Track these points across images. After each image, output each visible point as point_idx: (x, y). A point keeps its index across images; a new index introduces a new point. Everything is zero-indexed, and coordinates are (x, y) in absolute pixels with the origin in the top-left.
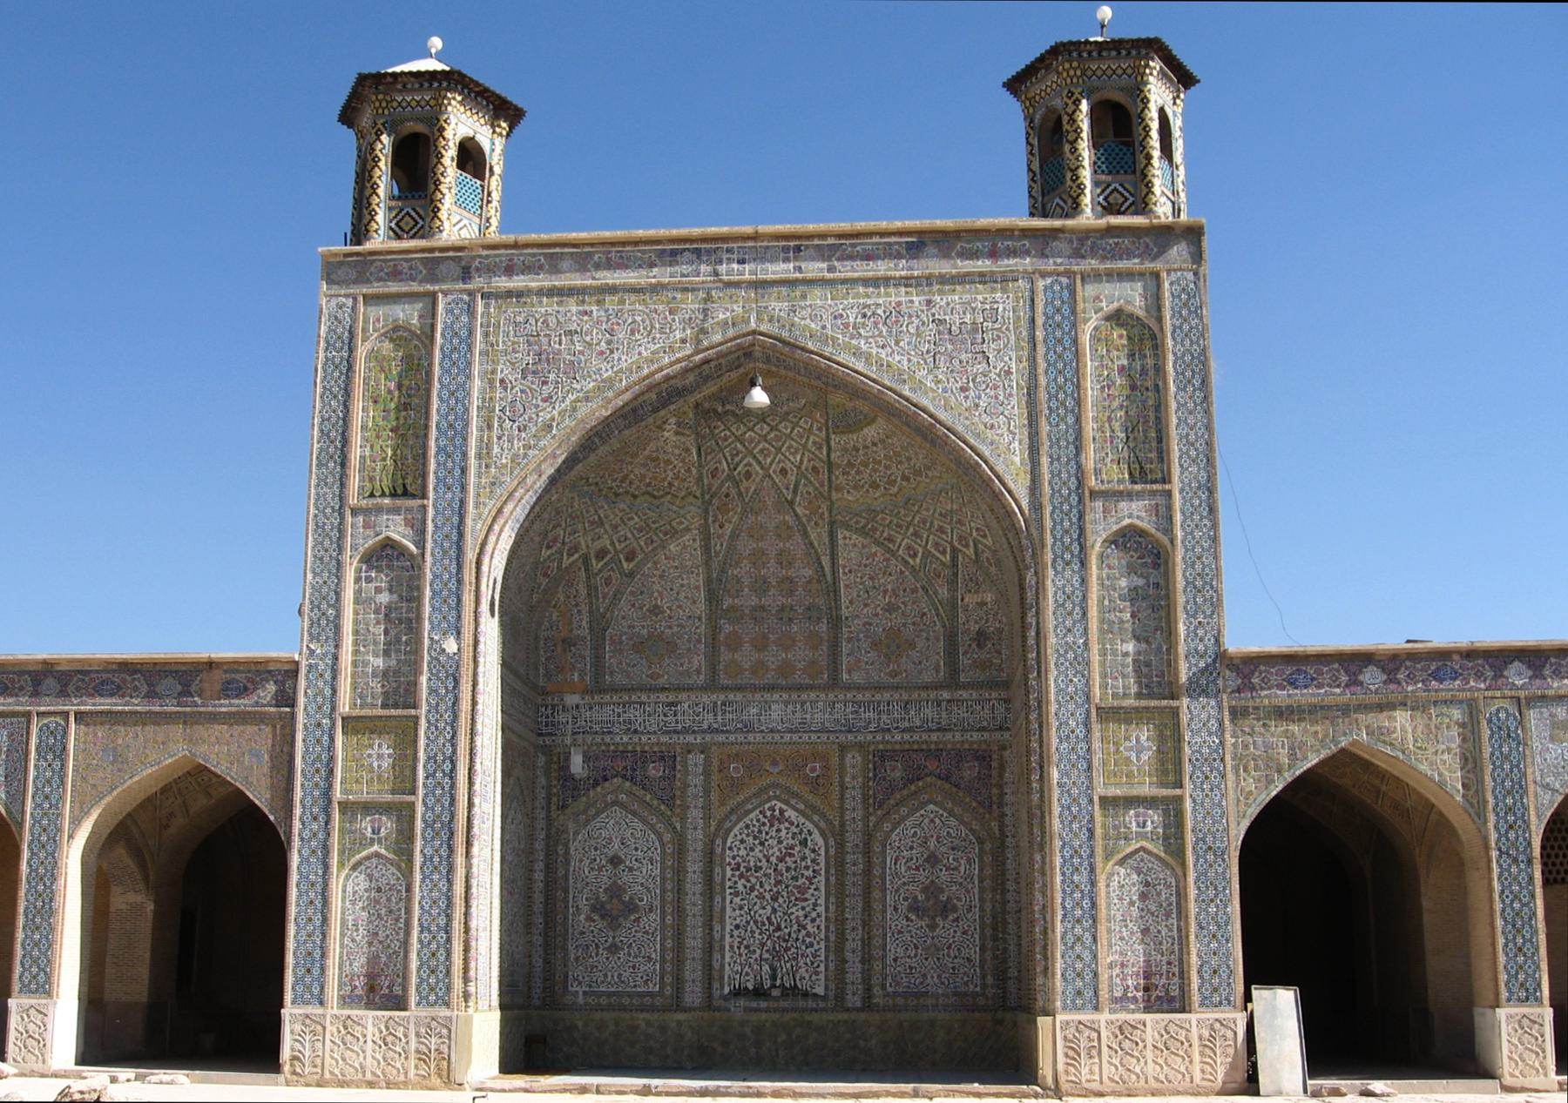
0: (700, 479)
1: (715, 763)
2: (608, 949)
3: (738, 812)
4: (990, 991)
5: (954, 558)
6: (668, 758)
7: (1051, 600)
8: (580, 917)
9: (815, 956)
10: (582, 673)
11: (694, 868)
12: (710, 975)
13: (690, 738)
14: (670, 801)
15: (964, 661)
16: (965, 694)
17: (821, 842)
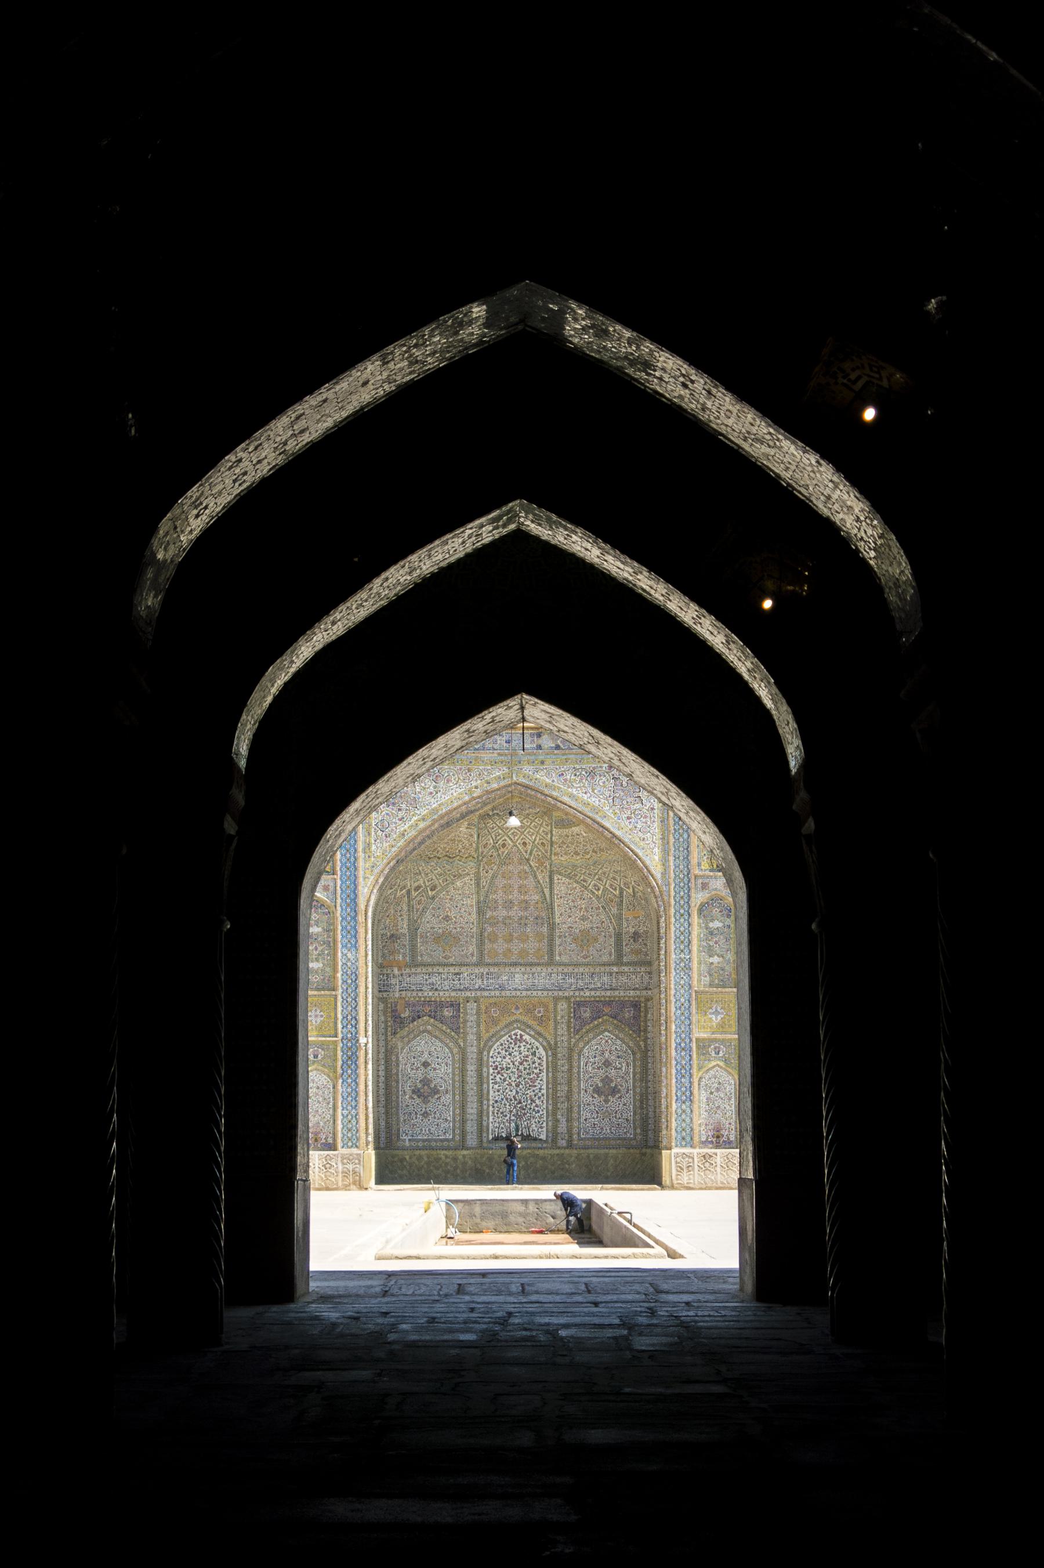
0: (477, 849)
1: (483, 1007)
2: (423, 1115)
3: (496, 1036)
4: (639, 1137)
5: (621, 893)
6: (455, 1005)
7: (673, 935)
8: (406, 1099)
9: (540, 1117)
10: (404, 957)
11: (471, 1068)
12: (481, 1129)
13: (468, 994)
14: (457, 1030)
15: (626, 949)
16: (626, 969)
17: (544, 1053)
